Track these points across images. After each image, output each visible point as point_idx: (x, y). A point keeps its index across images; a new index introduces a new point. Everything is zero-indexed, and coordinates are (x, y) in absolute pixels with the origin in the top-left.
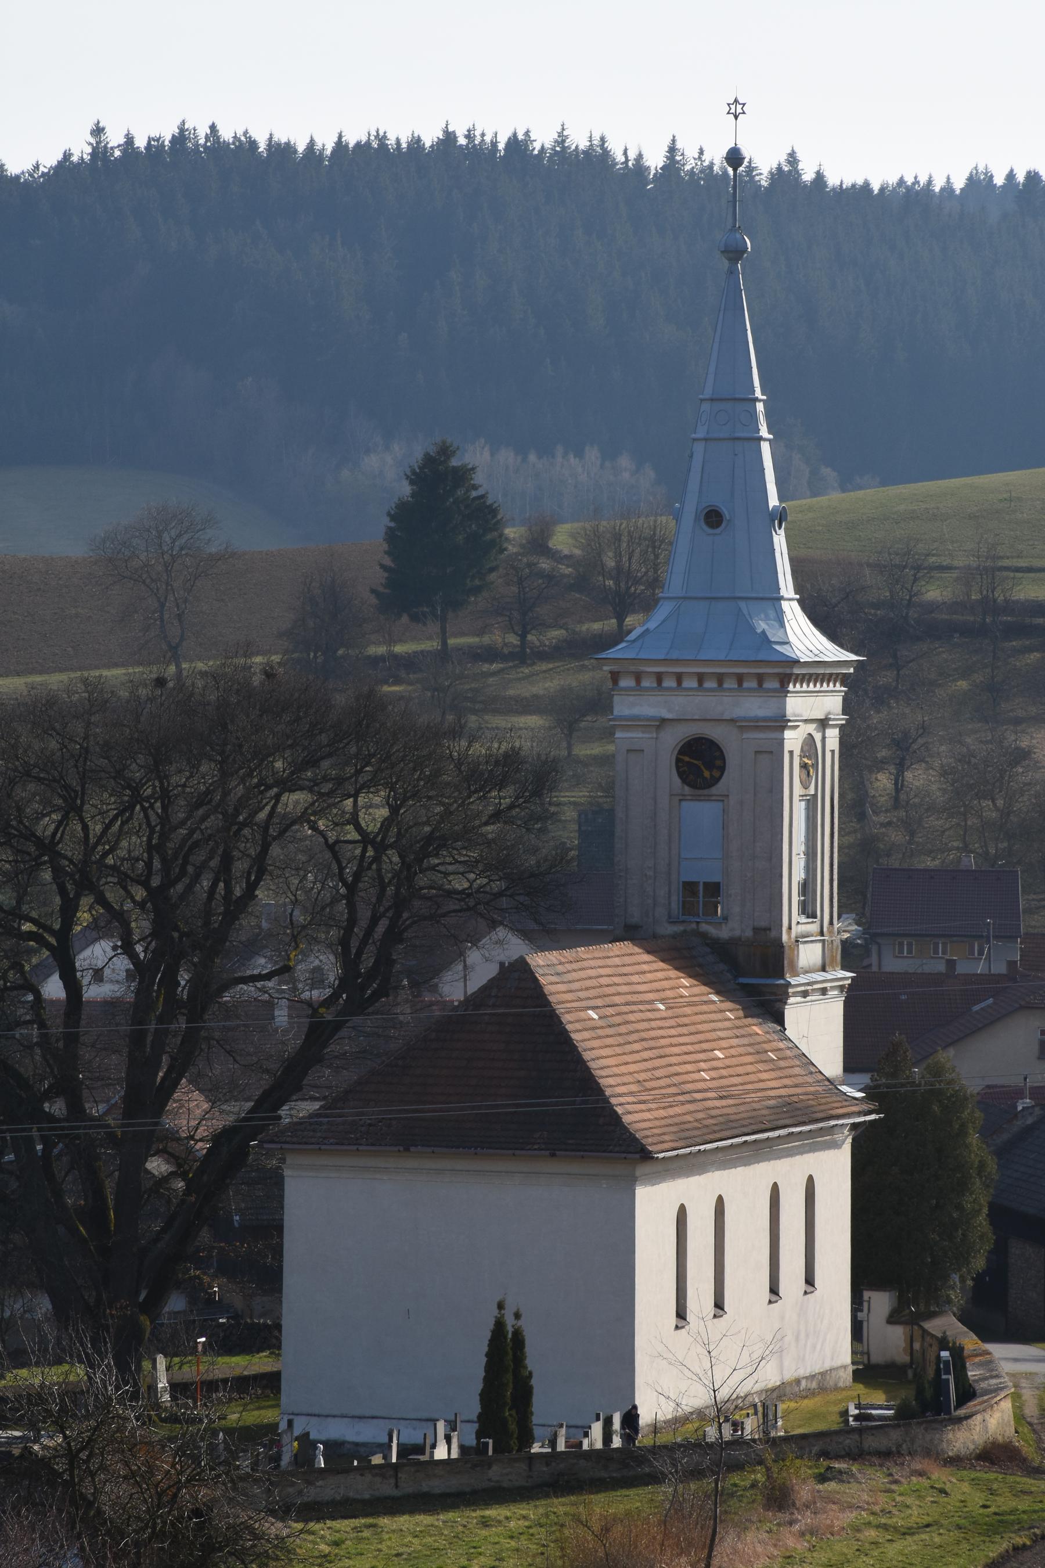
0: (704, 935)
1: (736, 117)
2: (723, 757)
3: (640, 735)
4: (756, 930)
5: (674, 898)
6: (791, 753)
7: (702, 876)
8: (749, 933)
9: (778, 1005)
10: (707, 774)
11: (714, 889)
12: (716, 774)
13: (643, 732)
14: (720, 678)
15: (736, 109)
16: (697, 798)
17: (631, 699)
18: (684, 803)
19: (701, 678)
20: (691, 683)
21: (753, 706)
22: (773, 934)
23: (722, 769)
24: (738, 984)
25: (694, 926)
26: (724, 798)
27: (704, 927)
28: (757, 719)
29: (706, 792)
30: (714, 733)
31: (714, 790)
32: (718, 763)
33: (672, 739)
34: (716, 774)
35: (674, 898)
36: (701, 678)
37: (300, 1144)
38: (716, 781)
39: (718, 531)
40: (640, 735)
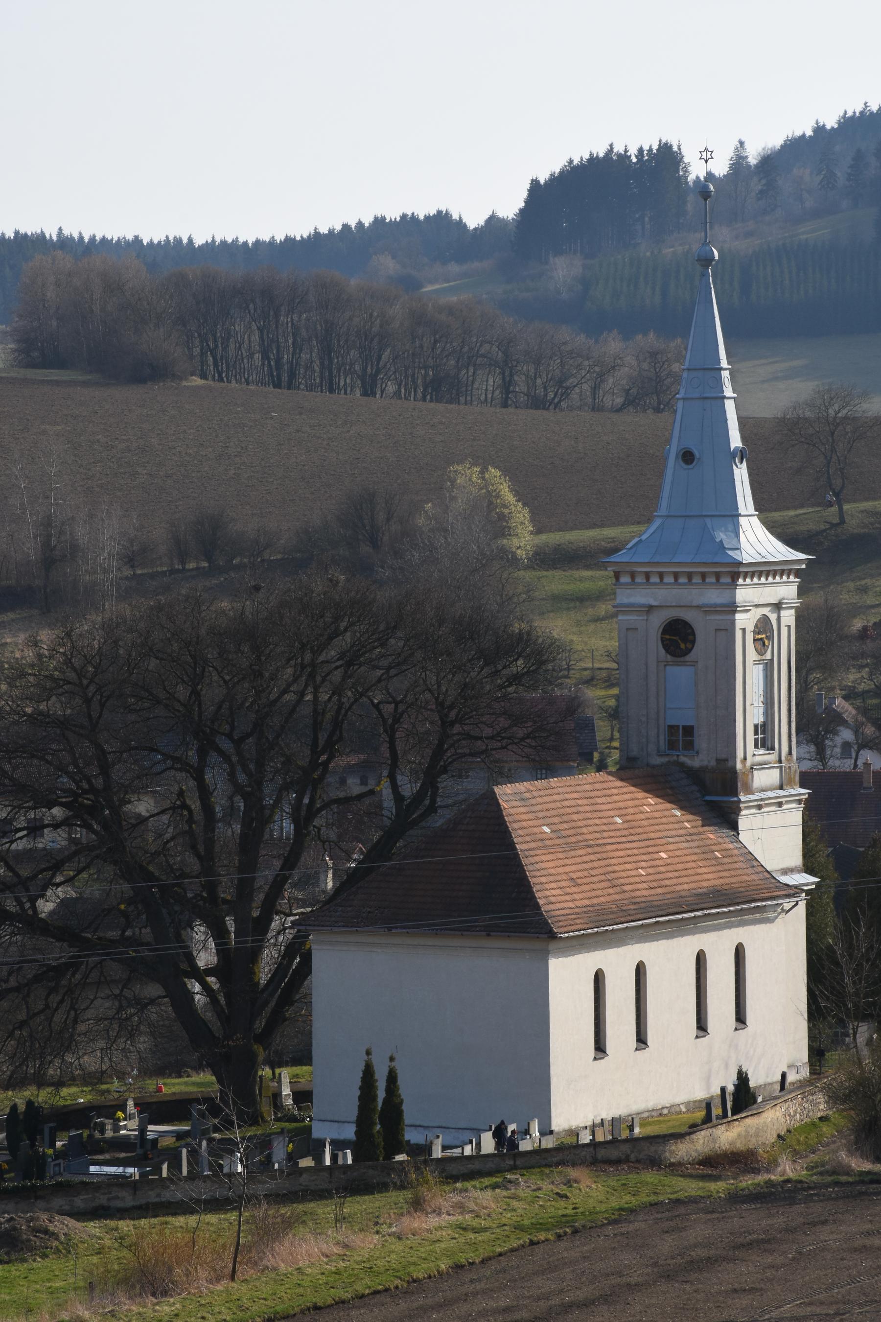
0: (682, 765)
1: (706, 161)
2: (693, 634)
3: (636, 618)
5: (662, 738)
6: (744, 630)
8: (713, 763)
9: (733, 816)
10: (683, 646)
11: (689, 731)
12: (689, 645)
13: (637, 616)
14: (690, 575)
16: (677, 664)
17: (629, 591)
18: (668, 668)
19: (676, 575)
21: (713, 596)
22: (730, 764)
23: (693, 642)
24: (704, 801)
25: (675, 758)
26: (694, 663)
27: (683, 759)
28: (716, 606)
29: (682, 659)
30: (688, 616)
31: (687, 658)
32: (691, 638)
33: (658, 621)
34: (689, 645)
36: (676, 575)
37: (318, 926)
38: (689, 651)
39: (691, 466)
40: (636, 618)
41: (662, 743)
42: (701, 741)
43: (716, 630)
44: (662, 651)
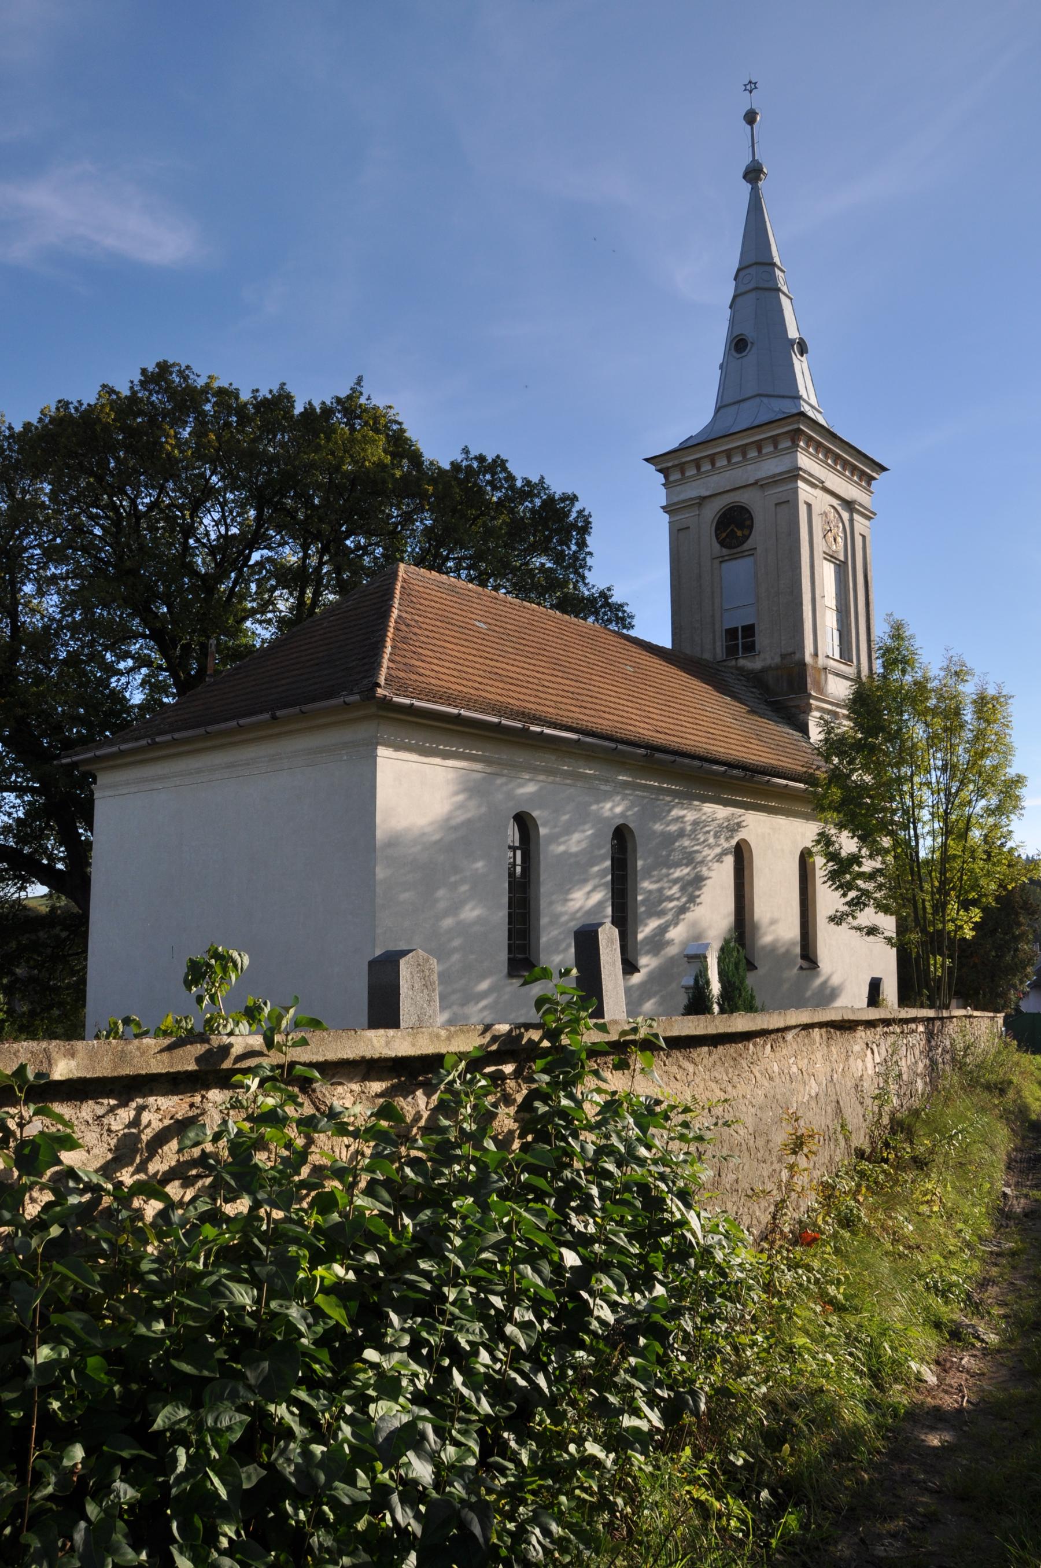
0: (741, 669)
2: (751, 519)
4: (783, 656)
5: (718, 644)
7: (739, 621)
8: (777, 660)
10: (739, 533)
11: (749, 630)
12: (746, 532)
15: (751, 86)
16: (733, 558)
17: (678, 488)
18: (724, 565)
20: (721, 462)
21: (772, 467)
22: (797, 656)
23: (751, 527)
27: (742, 662)
28: (774, 476)
29: (739, 549)
30: (743, 498)
31: (745, 547)
32: (748, 523)
33: (711, 512)
35: (718, 644)
41: (719, 650)
42: (761, 640)
43: (776, 504)
44: (716, 546)
